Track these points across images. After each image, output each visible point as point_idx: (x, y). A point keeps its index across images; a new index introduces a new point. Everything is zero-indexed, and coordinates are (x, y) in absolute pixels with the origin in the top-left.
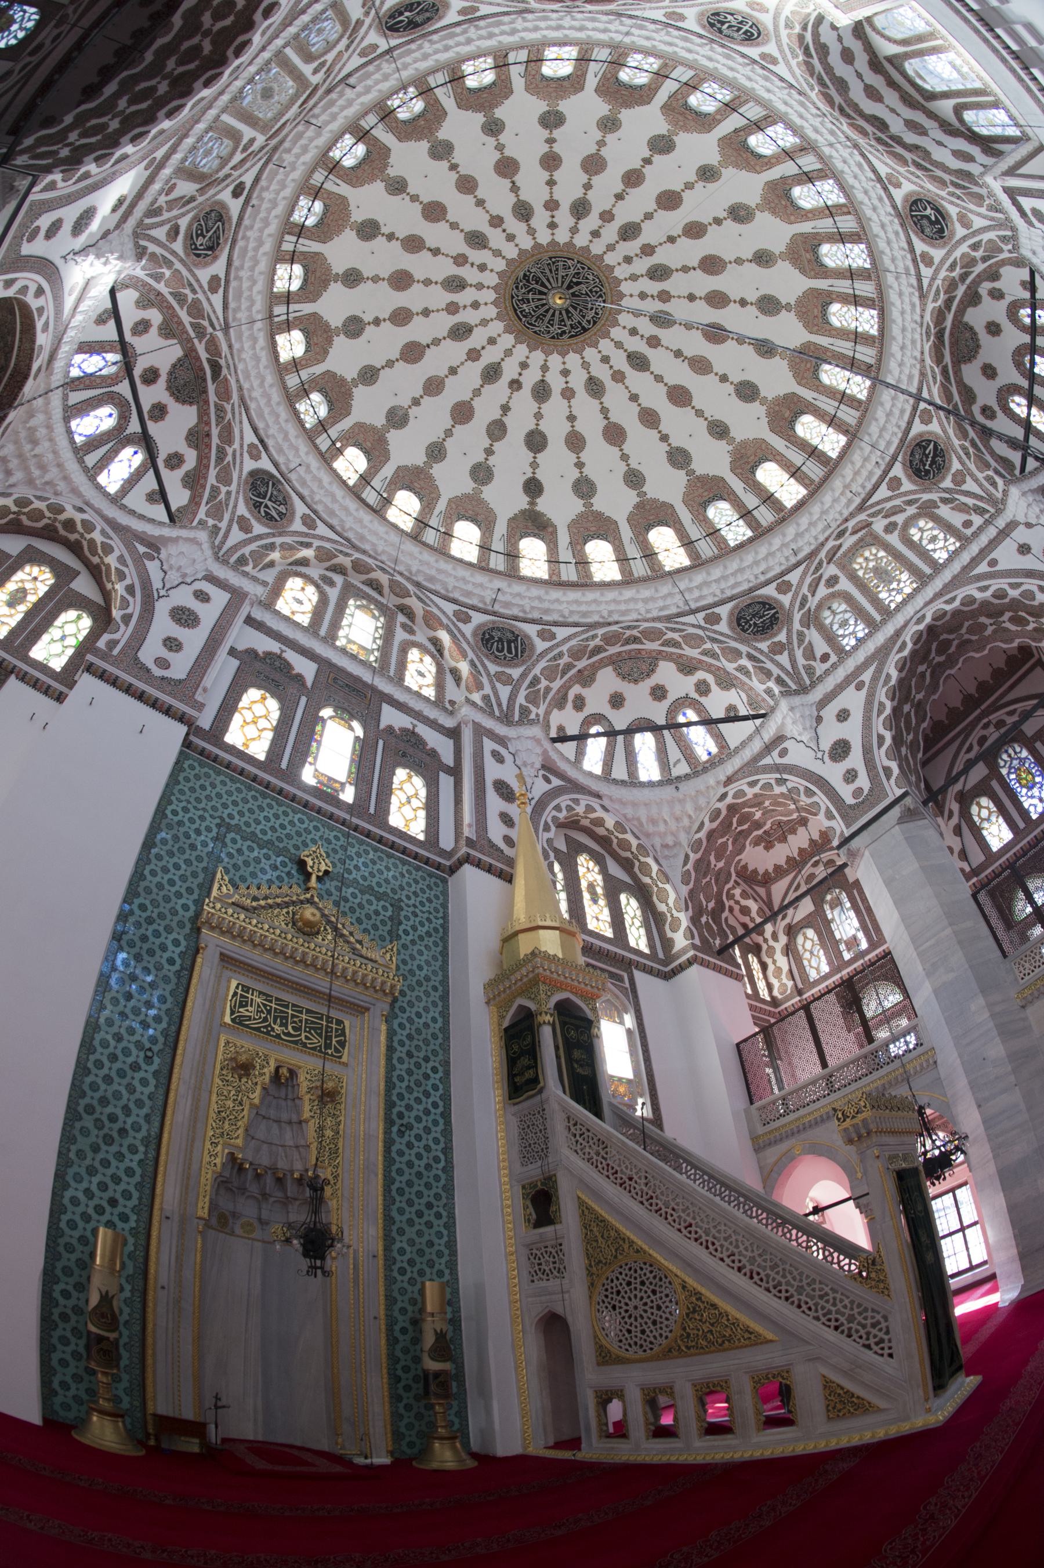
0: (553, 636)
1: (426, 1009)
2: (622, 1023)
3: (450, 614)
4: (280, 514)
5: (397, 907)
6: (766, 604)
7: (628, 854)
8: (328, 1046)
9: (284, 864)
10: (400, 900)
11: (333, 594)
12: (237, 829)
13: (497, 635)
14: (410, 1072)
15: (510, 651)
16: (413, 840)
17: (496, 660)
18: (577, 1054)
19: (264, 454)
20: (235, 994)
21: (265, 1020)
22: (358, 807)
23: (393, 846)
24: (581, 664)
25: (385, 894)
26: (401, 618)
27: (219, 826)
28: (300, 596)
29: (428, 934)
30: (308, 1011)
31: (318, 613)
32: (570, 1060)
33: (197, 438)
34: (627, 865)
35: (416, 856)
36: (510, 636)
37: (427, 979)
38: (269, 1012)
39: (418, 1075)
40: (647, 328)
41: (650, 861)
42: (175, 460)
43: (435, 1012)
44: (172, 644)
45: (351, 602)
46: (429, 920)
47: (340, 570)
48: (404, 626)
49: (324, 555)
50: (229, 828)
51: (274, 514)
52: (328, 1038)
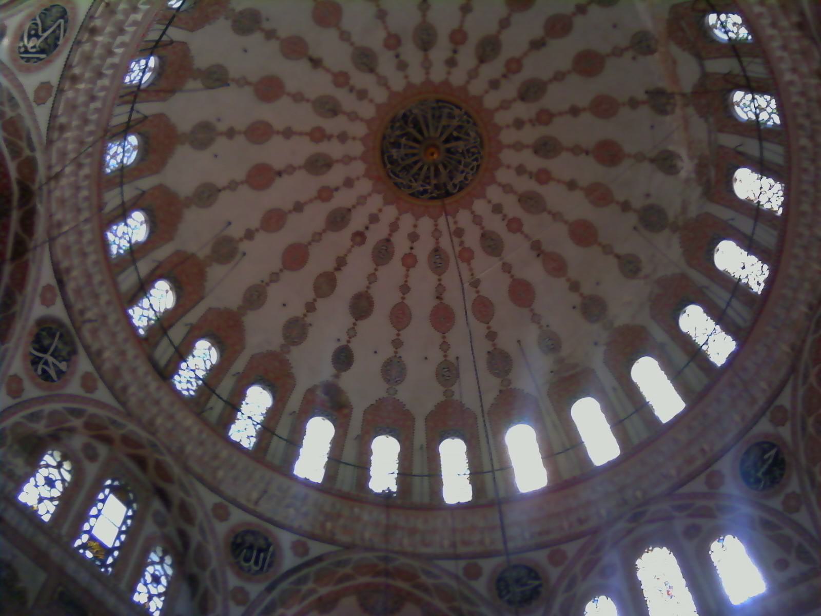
0: (306, 551)
3: (209, 506)
4: (60, 373)
6: (533, 572)
11: (92, 469)
13: (250, 539)
15: (256, 563)
17: (240, 571)
19: (59, 301)
24: (323, 591)
26: (157, 505)
28: (54, 474)
31: (65, 501)
36: (261, 543)
40: (513, 209)
45: (109, 482)
47: (107, 440)
48: (156, 514)
51: (53, 373)
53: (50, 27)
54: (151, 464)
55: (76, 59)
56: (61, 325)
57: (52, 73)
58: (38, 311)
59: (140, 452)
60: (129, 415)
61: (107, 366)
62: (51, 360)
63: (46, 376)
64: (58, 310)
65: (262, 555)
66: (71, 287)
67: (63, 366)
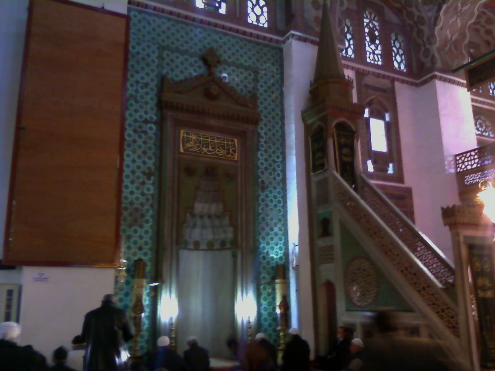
1: (273, 127)
2: (383, 118)
5: (256, 72)
7: (398, 5)
8: (228, 153)
9: (196, 62)
10: (258, 68)
12: (168, 48)
14: (266, 160)
16: (262, 29)
18: (345, 151)
20: (184, 137)
21: (199, 146)
22: (228, 17)
23: (251, 35)
25: (249, 66)
27: (158, 48)
29: (273, 85)
30: (218, 138)
32: (341, 154)
34: (398, 12)
35: (265, 38)
37: (273, 110)
38: (200, 142)
39: (270, 161)
41: (414, 10)
43: (278, 127)
46: (273, 76)
52: (228, 149)
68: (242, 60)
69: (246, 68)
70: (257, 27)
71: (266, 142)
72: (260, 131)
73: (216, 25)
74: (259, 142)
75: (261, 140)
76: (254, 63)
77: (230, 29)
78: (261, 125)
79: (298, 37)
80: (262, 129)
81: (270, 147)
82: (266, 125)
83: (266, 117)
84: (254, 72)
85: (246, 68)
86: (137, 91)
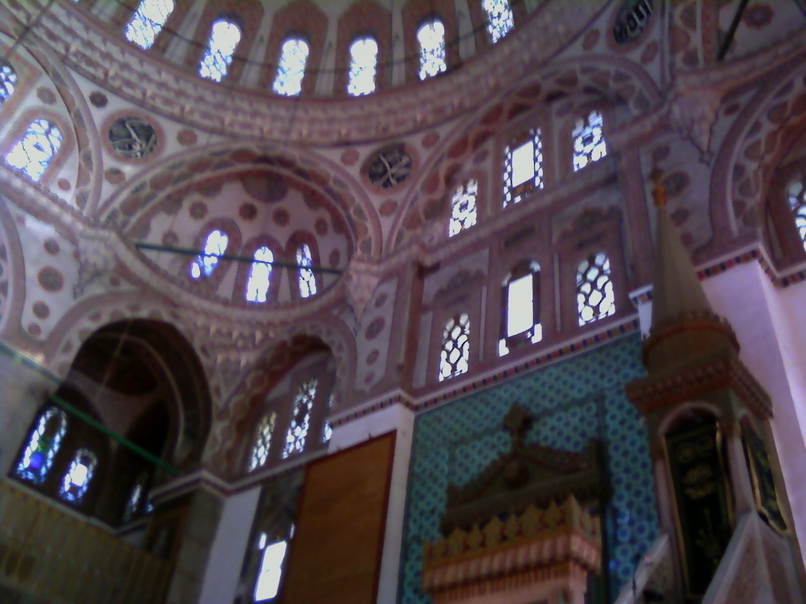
4: (408, 166)
12: (463, 441)
13: (623, 18)
15: (641, 16)
33: (313, 200)
42: (321, 226)
44: (373, 357)
49: (459, 148)
50: (454, 444)
51: (403, 171)
53: (129, 132)
54: (520, 100)
55: (167, 109)
56: (377, 154)
57: (171, 130)
58: (354, 170)
59: (506, 108)
60: (474, 108)
61: (430, 119)
62: (394, 170)
63: (400, 179)
64: (364, 152)
65: (641, 8)
66: (355, 136)
67: (405, 160)
68: (575, 394)
69: (581, 403)
70: (598, 323)
71: (631, 523)
72: (617, 504)
73: (527, 366)
74: (617, 526)
75: (619, 521)
76: (595, 386)
77: (549, 357)
78: (620, 490)
79: (646, 297)
80: (621, 498)
81: (641, 529)
82: (628, 487)
83: (627, 470)
84: (596, 401)
85: (581, 403)
86: (421, 527)
